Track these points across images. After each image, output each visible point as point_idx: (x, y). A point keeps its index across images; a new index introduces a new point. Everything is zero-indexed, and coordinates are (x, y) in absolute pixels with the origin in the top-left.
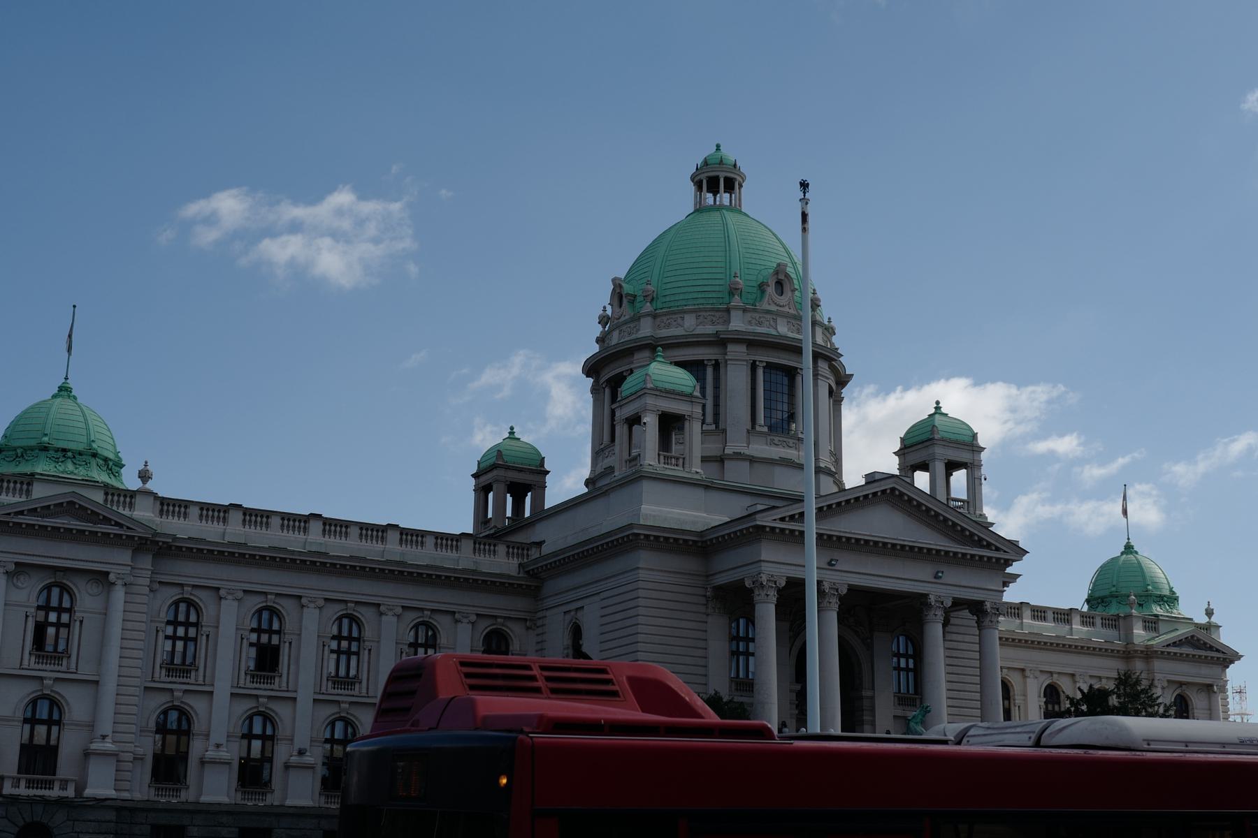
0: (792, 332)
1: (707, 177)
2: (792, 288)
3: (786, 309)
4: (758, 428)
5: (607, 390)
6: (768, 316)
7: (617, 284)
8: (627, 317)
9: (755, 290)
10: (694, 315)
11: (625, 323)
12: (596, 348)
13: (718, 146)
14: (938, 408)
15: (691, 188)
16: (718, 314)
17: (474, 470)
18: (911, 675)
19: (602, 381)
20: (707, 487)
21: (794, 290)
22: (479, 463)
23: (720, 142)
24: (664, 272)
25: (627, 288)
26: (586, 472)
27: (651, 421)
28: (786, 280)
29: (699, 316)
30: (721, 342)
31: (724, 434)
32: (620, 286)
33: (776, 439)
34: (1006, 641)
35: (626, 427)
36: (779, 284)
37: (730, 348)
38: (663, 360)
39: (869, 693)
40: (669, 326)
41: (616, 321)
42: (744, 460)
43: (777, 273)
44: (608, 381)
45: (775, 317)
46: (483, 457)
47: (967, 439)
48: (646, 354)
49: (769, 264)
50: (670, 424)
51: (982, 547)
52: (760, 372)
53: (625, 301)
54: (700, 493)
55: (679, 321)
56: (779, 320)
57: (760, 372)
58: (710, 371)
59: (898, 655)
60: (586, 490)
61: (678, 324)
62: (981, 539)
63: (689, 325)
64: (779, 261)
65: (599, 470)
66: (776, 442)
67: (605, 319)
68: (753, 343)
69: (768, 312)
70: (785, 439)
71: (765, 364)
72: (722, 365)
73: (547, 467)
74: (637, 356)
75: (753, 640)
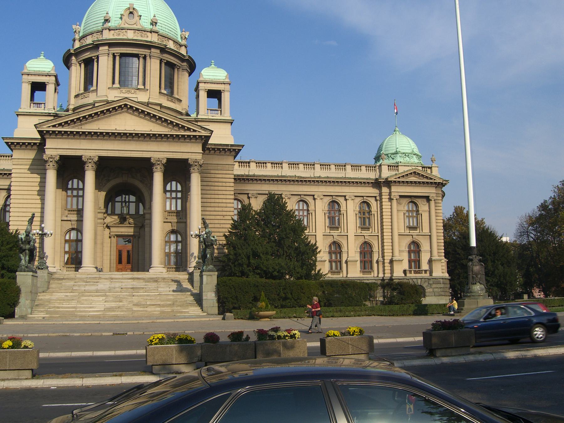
3: (135, 27)
4: (114, 86)
6: (124, 30)
18: (179, 201)
28: (134, 11)
30: (96, 47)
33: (124, 90)
34: (239, 179)
37: (101, 48)
38: (43, 57)
39: (149, 212)
51: (185, 130)
52: (117, 58)
56: (129, 31)
57: (117, 58)
59: (177, 191)
62: (183, 127)
63: (89, 40)
64: (128, 3)
66: (124, 92)
68: (111, 45)
70: (128, 90)
71: (119, 54)
75: (83, 189)
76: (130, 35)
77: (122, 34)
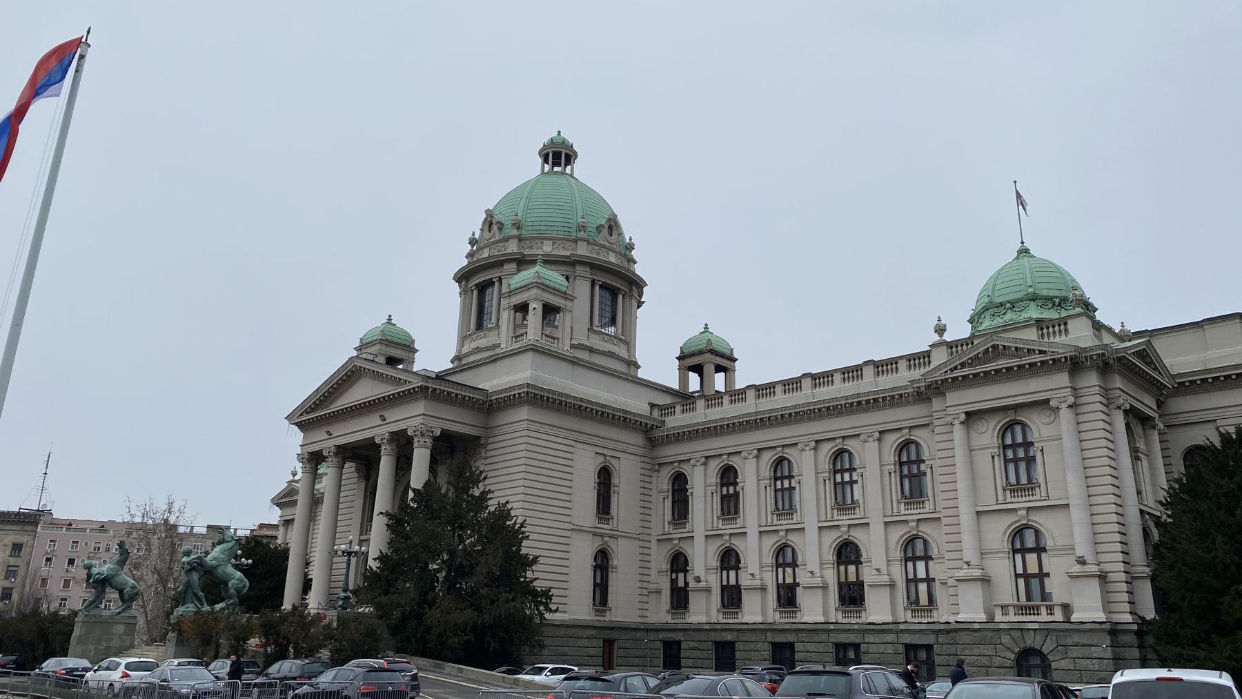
3: (614, 246)
5: (475, 292)
7: (489, 214)
8: (497, 238)
9: (595, 230)
11: (494, 243)
12: (465, 262)
13: (559, 132)
14: (706, 328)
15: (540, 160)
16: (568, 244)
17: (357, 344)
19: (470, 286)
20: (573, 363)
22: (361, 340)
23: (561, 130)
25: (497, 218)
26: (453, 353)
27: (536, 309)
32: (492, 216)
35: (512, 312)
36: (610, 228)
37: (578, 268)
40: (531, 247)
41: (486, 242)
42: (587, 349)
43: (609, 220)
44: (477, 285)
46: (365, 335)
47: (728, 352)
48: (514, 266)
49: (605, 215)
50: (550, 311)
52: (597, 288)
53: (495, 227)
54: (570, 366)
55: (539, 244)
57: (597, 288)
60: (451, 366)
65: (465, 350)
67: (474, 241)
68: (595, 266)
69: (602, 246)
71: (601, 283)
73: (416, 346)
74: (506, 267)
76: (612, 258)
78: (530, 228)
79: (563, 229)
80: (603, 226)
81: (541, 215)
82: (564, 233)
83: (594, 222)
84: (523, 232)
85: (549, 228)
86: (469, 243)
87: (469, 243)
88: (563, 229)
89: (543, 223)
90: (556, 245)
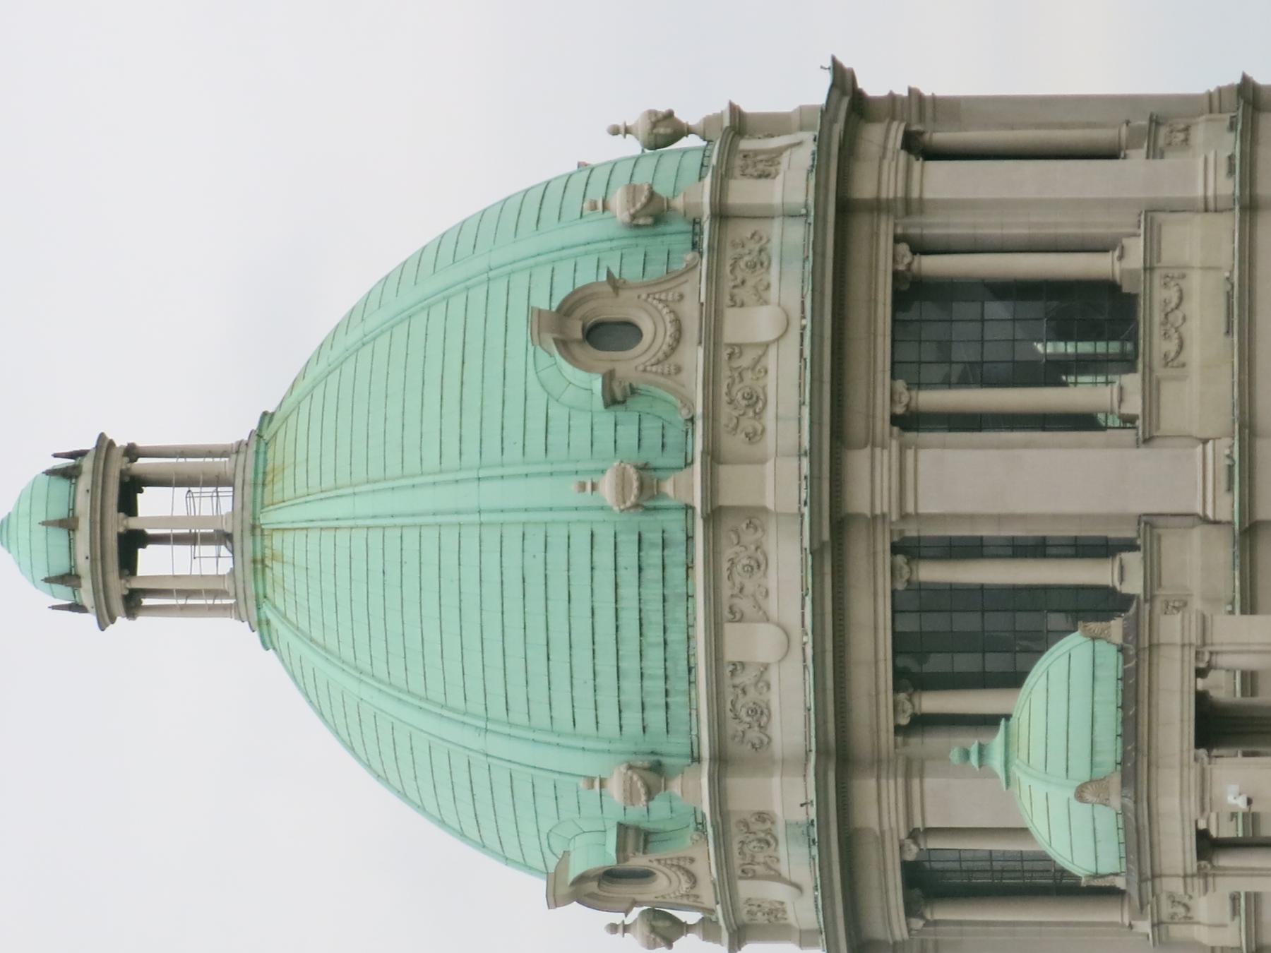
0: (768, 287)
1: (121, 577)
2: (609, 289)
3: (690, 311)
10: (730, 629)
11: (724, 861)
16: (728, 552)
21: (615, 284)
24: (510, 725)
28: (579, 312)
29: (732, 611)
31: (1161, 521)
33: (1162, 346)
40: (760, 713)
43: (564, 345)
45: (725, 356)
55: (745, 678)
58: (933, 573)
61: (756, 684)
66: (1172, 347)
70: (1158, 317)
71: (900, 385)
72: (912, 531)
74: (867, 816)
77: (748, 376)
78: (656, 718)
79: (653, 573)
80: (609, 378)
81: (584, 673)
82: (677, 573)
83: (581, 422)
84: (675, 746)
85: (654, 635)
86: (669, 944)
87: (669, 944)
88: (653, 573)
89: (630, 664)
90: (744, 604)
